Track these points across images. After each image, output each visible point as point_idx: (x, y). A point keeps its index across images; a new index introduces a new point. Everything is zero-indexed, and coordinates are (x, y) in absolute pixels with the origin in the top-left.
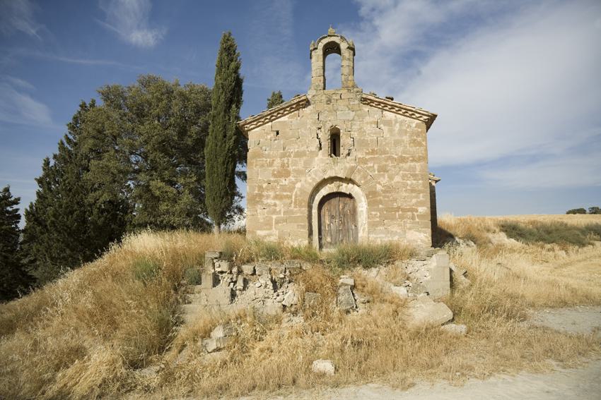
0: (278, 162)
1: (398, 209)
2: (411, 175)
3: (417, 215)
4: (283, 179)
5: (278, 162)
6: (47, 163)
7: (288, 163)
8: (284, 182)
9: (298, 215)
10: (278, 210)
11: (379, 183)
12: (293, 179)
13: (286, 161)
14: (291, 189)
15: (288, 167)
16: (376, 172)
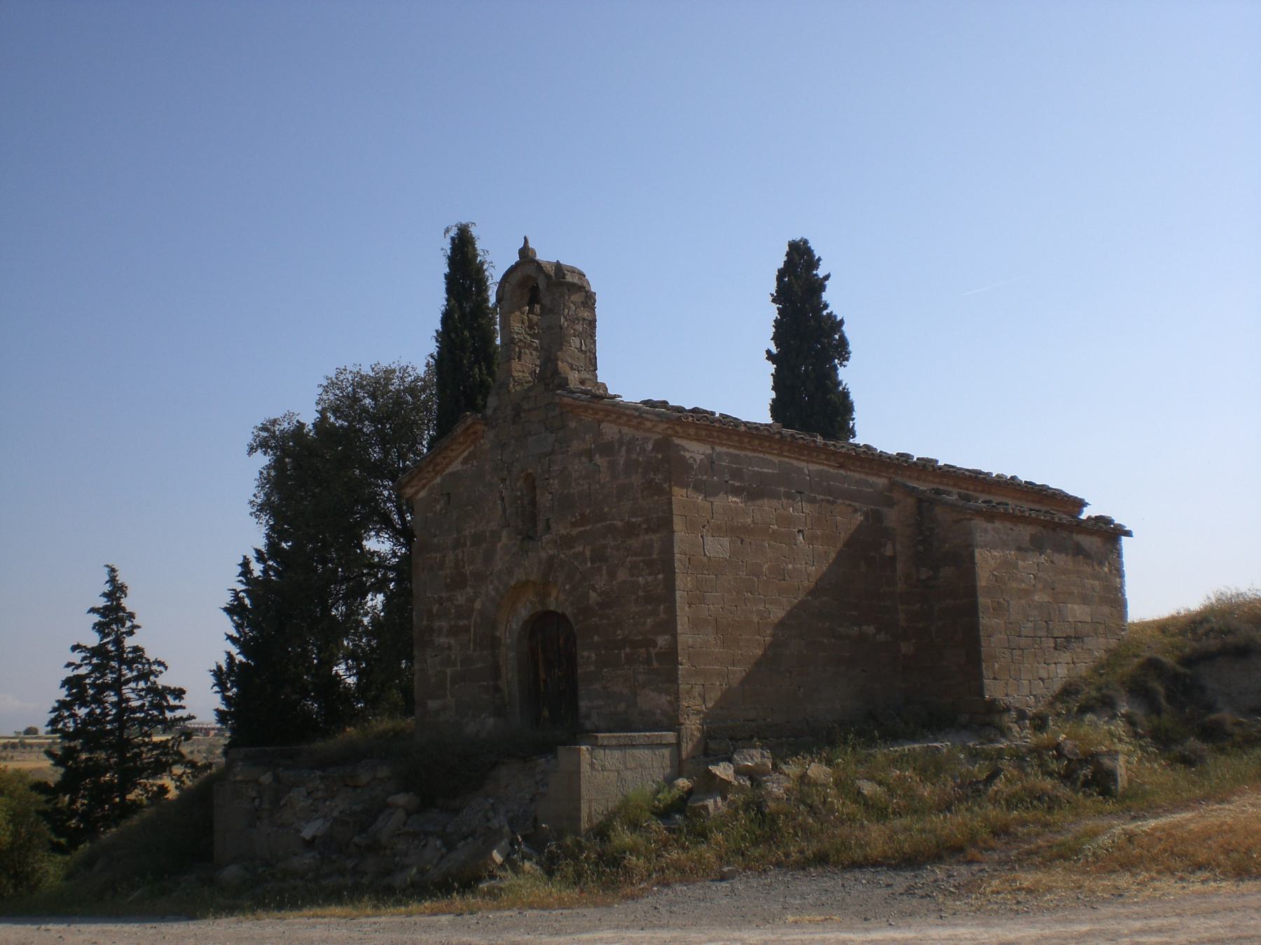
3: (657, 654)
6: (245, 564)
8: (461, 599)
9: (479, 665)
11: (594, 590)
16: (589, 564)
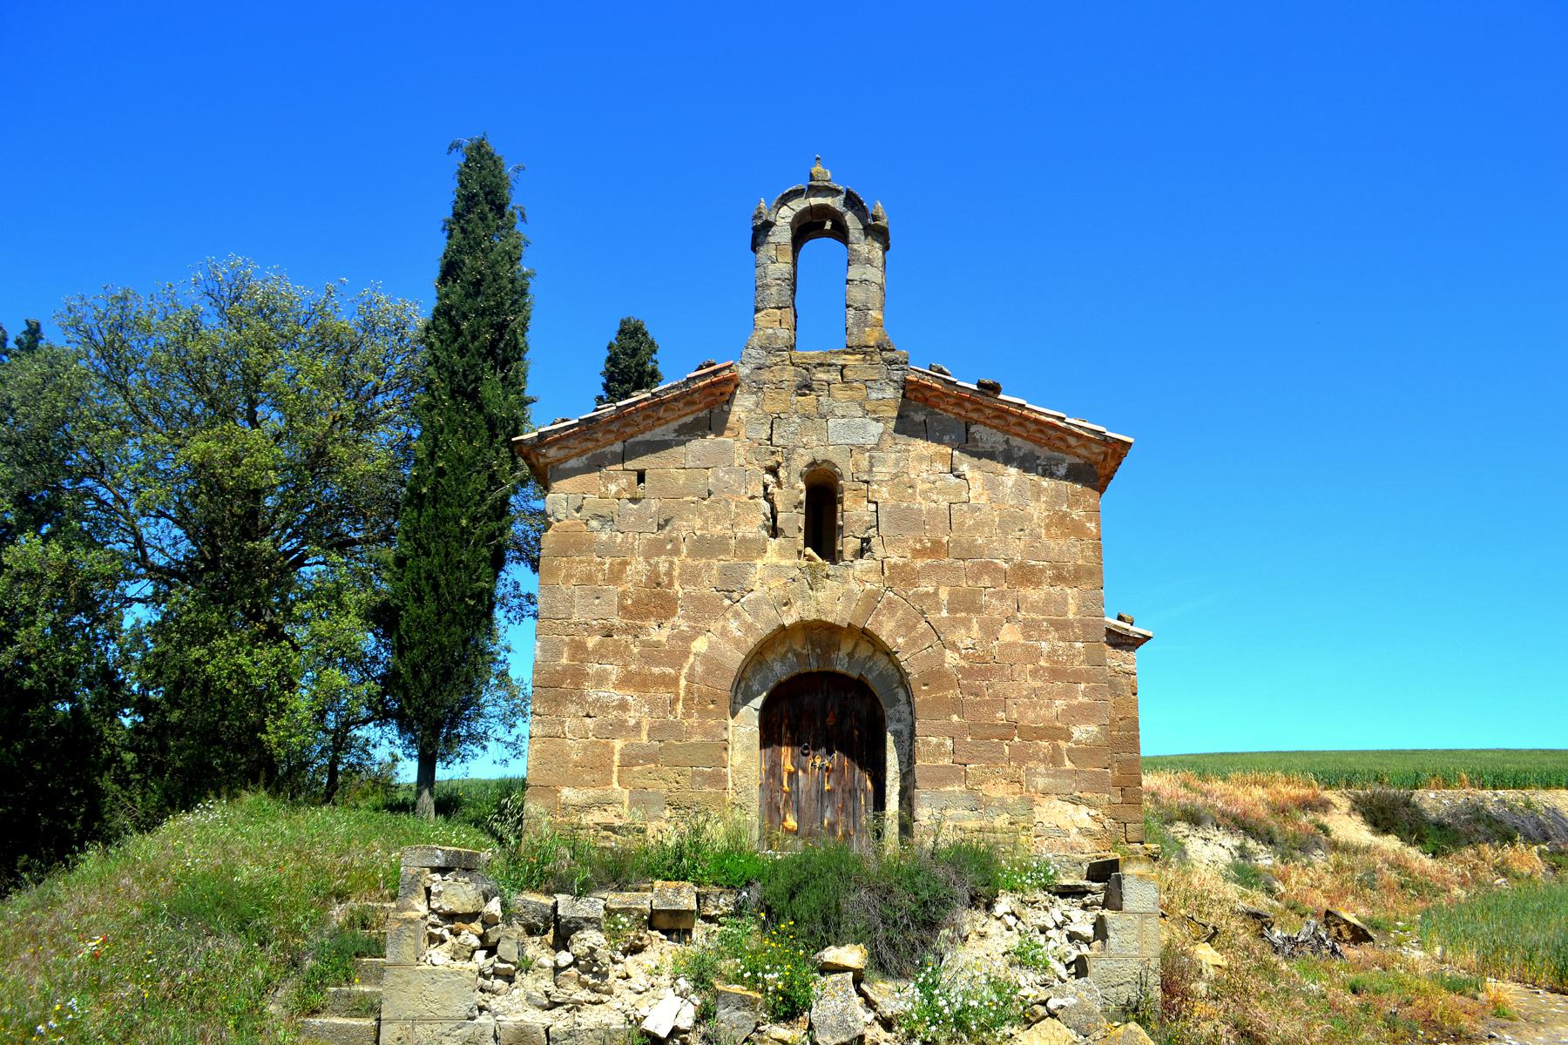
0: (638, 567)
1: (1014, 726)
2: (1052, 623)
3: (1070, 750)
4: (652, 623)
5: (638, 567)
7: (669, 574)
8: (659, 634)
9: (696, 739)
10: (632, 722)
11: (954, 647)
12: (684, 625)
13: (663, 568)
14: (677, 656)
15: (671, 584)
16: (944, 613)
